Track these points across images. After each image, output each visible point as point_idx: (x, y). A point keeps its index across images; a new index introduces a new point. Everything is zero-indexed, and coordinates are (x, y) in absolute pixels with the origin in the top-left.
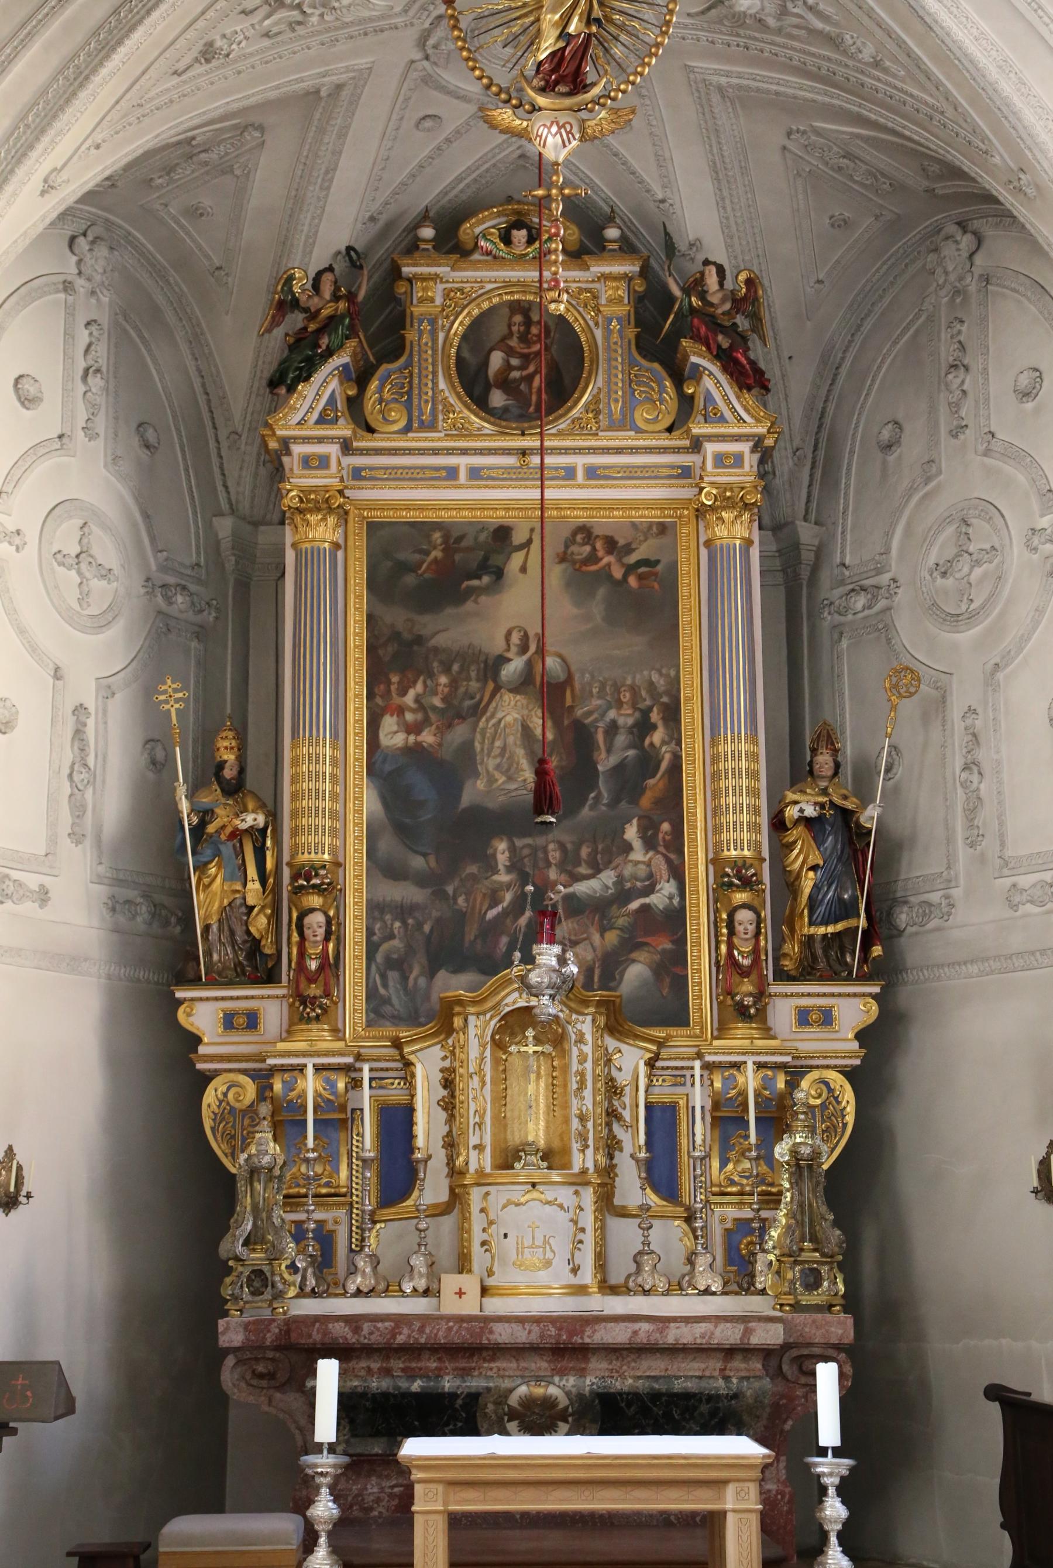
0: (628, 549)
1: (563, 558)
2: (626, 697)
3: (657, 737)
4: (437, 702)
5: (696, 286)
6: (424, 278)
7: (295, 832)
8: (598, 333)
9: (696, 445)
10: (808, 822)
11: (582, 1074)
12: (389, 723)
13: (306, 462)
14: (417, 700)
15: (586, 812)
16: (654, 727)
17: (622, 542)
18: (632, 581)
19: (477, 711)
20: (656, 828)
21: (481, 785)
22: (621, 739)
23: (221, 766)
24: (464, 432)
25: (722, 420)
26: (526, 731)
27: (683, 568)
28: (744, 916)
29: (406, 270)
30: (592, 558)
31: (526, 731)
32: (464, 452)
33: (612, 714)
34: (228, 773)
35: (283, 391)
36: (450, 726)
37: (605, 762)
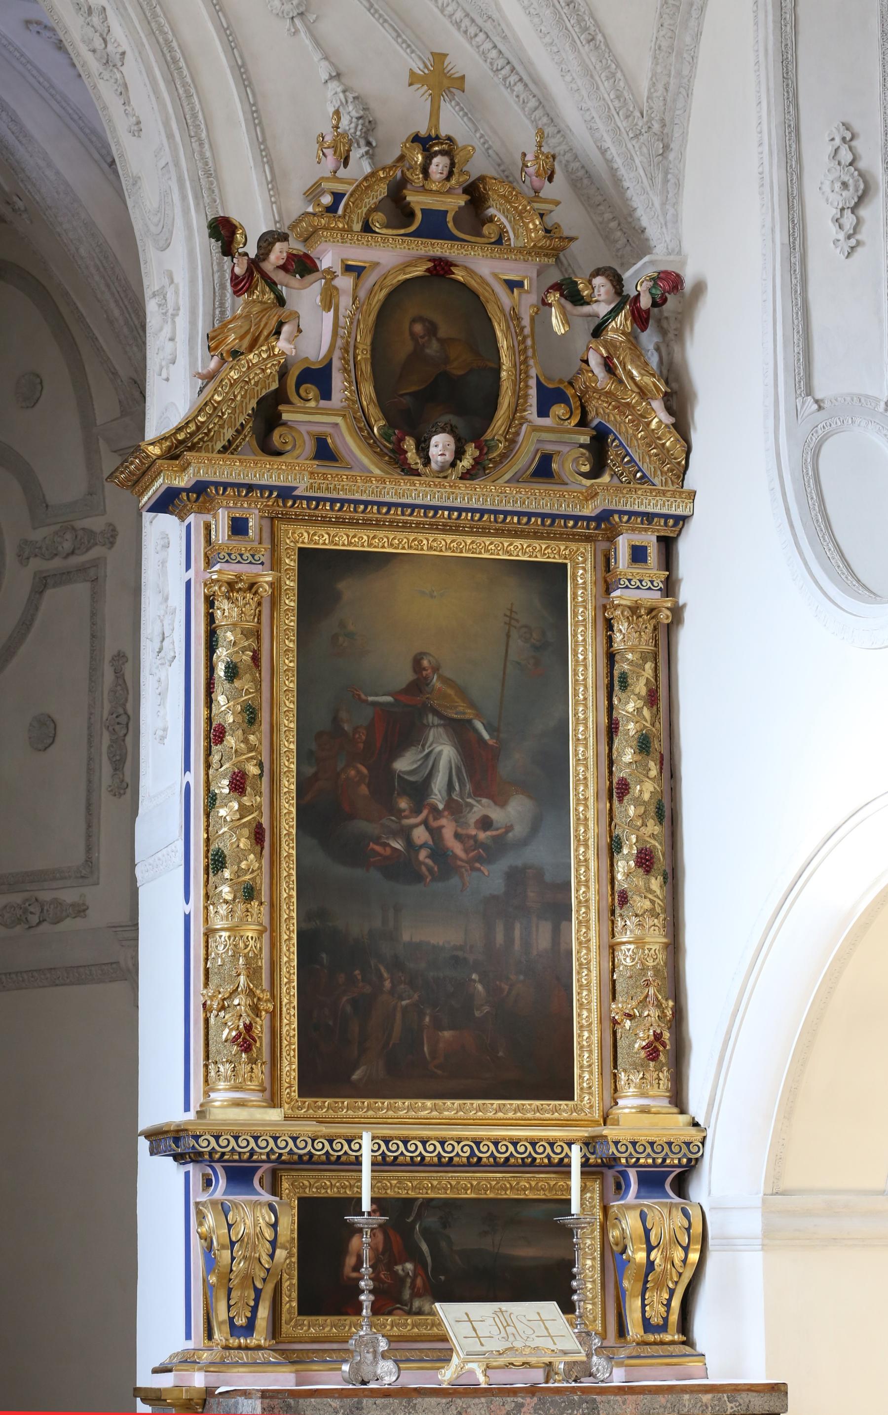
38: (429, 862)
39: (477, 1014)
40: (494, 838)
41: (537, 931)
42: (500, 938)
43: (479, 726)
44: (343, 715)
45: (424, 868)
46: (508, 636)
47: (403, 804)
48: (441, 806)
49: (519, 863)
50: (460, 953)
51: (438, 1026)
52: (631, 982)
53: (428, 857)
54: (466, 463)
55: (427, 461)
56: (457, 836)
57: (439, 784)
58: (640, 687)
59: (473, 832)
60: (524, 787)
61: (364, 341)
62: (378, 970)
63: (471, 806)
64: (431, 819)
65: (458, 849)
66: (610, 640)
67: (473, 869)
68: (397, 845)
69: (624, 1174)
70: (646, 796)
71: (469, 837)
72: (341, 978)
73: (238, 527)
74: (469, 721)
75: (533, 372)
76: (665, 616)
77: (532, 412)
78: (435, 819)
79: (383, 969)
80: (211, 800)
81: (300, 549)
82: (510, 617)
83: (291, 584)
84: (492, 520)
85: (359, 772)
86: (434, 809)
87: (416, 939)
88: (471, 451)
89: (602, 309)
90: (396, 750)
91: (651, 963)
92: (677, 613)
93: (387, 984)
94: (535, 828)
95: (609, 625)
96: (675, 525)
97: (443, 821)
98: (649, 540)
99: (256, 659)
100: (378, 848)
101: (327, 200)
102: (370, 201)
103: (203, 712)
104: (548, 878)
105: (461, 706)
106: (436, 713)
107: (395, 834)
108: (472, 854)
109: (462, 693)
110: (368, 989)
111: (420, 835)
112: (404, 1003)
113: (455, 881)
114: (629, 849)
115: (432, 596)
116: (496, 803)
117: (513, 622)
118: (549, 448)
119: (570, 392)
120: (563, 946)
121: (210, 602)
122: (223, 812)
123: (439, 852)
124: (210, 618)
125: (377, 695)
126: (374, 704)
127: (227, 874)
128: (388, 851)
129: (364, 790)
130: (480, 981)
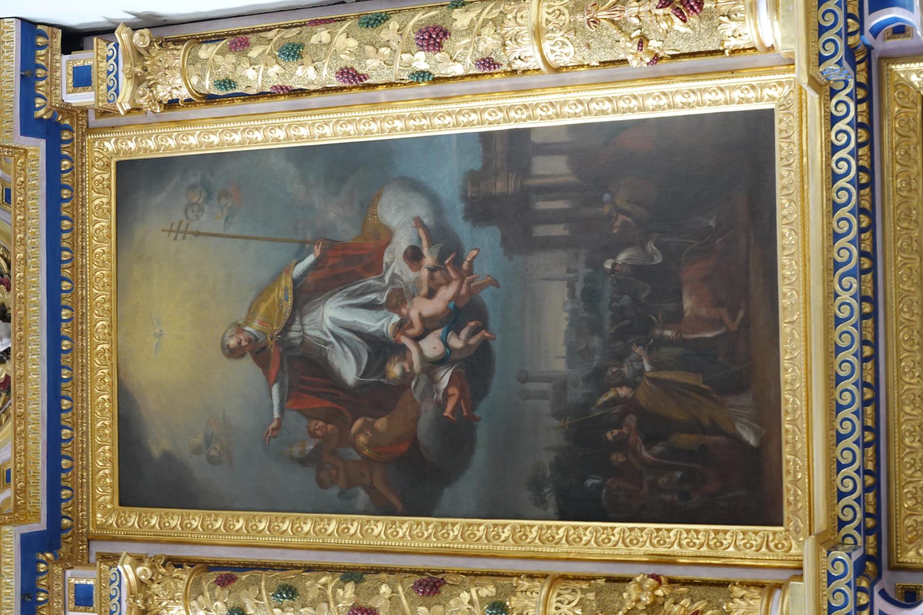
38: (464, 333)
39: (658, 259)
40: (431, 244)
41: (543, 176)
42: (558, 230)
44: (296, 451)
45: (473, 341)
46: (197, 234)
47: (395, 370)
48: (396, 318)
49: (460, 206)
50: (579, 287)
51: (676, 317)
52: (594, 44)
53: (458, 334)
56: (431, 295)
57: (372, 322)
59: (424, 273)
60: (368, 205)
62: (605, 405)
63: (394, 275)
64: (411, 332)
65: (446, 294)
67: (470, 272)
68: (445, 377)
69: (875, 32)
70: (353, 43)
71: (431, 278)
72: (618, 458)
74: (295, 282)
76: (141, 39)
78: (411, 326)
79: (604, 399)
82: (178, 232)
84: (69, 265)
85: (361, 431)
86: (403, 326)
87: (563, 350)
91: (566, 18)
93: (624, 392)
94: (415, 186)
95: (172, 104)
96: (43, 34)
97: (414, 315)
98: (66, 64)
100: (449, 408)
104: (477, 165)
105: (279, 293)
106: (287, 328)
107: (433, 382)
108: (453, 274)
109: (263, 293)
110: (631, 420)
111: (432, 346)
112: (647, 367)
113: (486, 296)
114: (421, 61)
115: (160, 335)
116: (388, 243)
117: (183, 228)
120: (563, 138)
125: (272, 406)
126: (282, 411)
128: (454, 390)
129: (381, 424)
130: (614, 257)
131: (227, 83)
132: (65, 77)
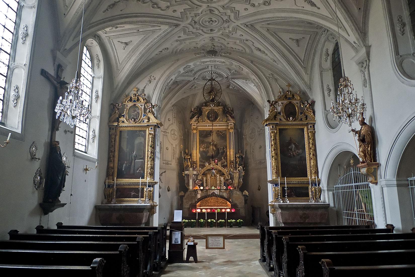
0: (222, 132)
1: (217, 133)
2: (222, 146)
3: (225, 149)
4: (205, 146)
5: (228, 109)
6: (204, 108)
7: (193, 158)
8: (219, 113)
9: (228, 123)
10: (238, 157)
11: (218, 180)
12: (201, 148)
13: (193, 125)
14: (203, 146)
15: (219, 156)
16: (225, 149)
17: (222, 132)
18: (223, 135)
19: (209, 147)
20: (225, 157)
21: (209, 154)
22: (222, 150)
23: (186, 152)
24: (208, 122)
25: (231, 121)
26: (213, 149)
27: (227, 134)
28: (232, 165)
29: (202, 108)
30: (219, 133)
31: (213, 149)
32: (208, 124)
33: (221, 147)
34: (187, 153)
35: (191, 119)
36: (206, 149)
37: (220, 152)
43: (297, 143)
47: (290, 151)
54: (294, 120)
55: (290, 120)
56: (295, 154)
57: (293, 149)
58: (312, 139)
59: (297, 153)
61: (283, 110)
65: (295, 154)
66: (309, 135)
68: (290, 155)
73: (273, 127)
75: (300, 111)
77: (300, 115)
80: (272, 151)
81: (279, 129)
83: (278, 132)
88: (294, 118)
89: (306, 105)
90: (289, 146)
91: (314, 164)
92: (315, 132)
94: (303, 152)
97: (294, 152)
99: (275, 139)
101: (279, 97)
102: (283, 97)
103: (271, 144)
106: (293, 142)
111: (292, 154)
114: (312, 154)
118: (301, 118)
119: (303, 112)
121: (271, 134)
122: (273, 152)
123: (293, 155)
124: (271, 135)
127: (274, 158)
131: (310, 139)
132: (311, 125)
